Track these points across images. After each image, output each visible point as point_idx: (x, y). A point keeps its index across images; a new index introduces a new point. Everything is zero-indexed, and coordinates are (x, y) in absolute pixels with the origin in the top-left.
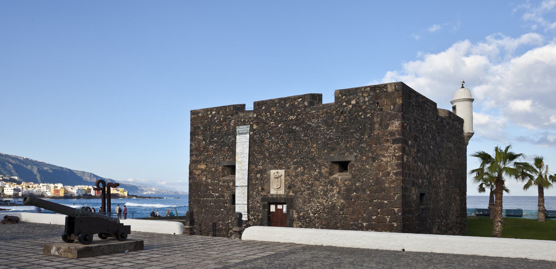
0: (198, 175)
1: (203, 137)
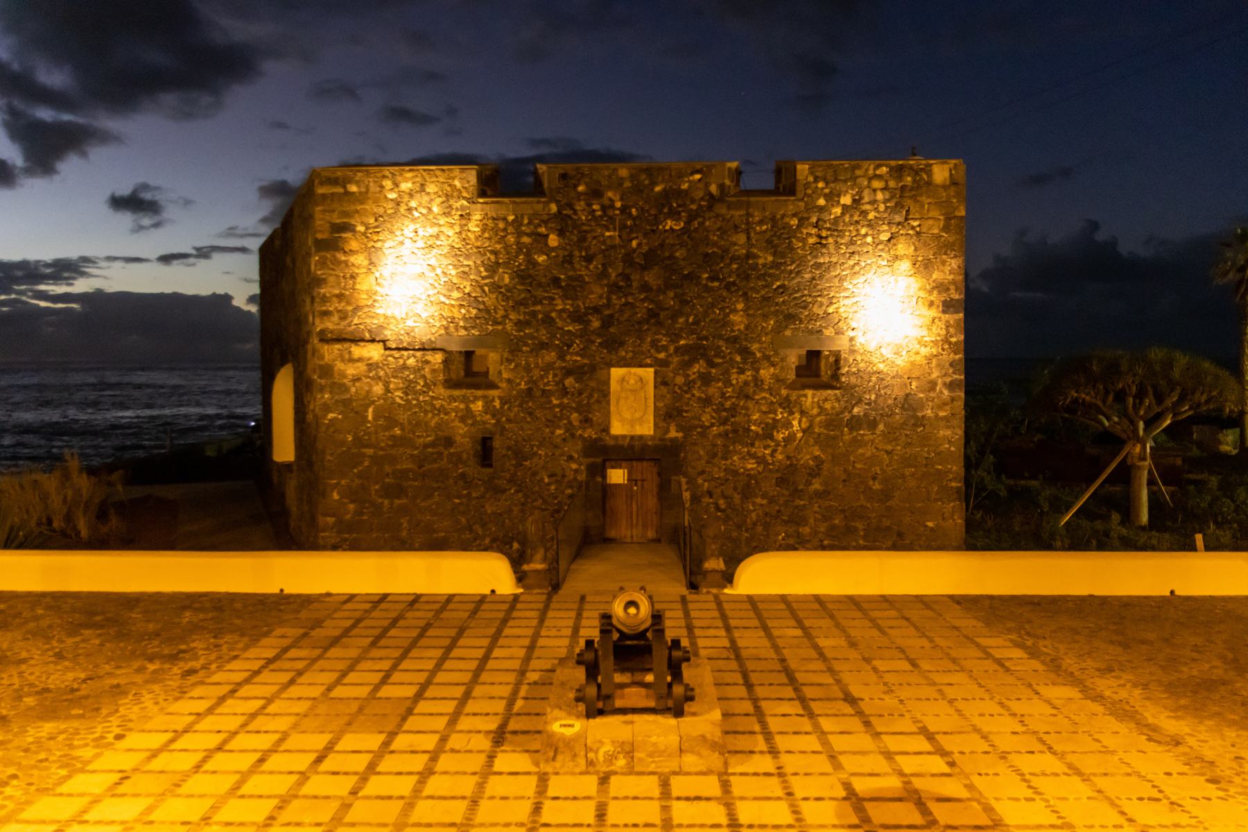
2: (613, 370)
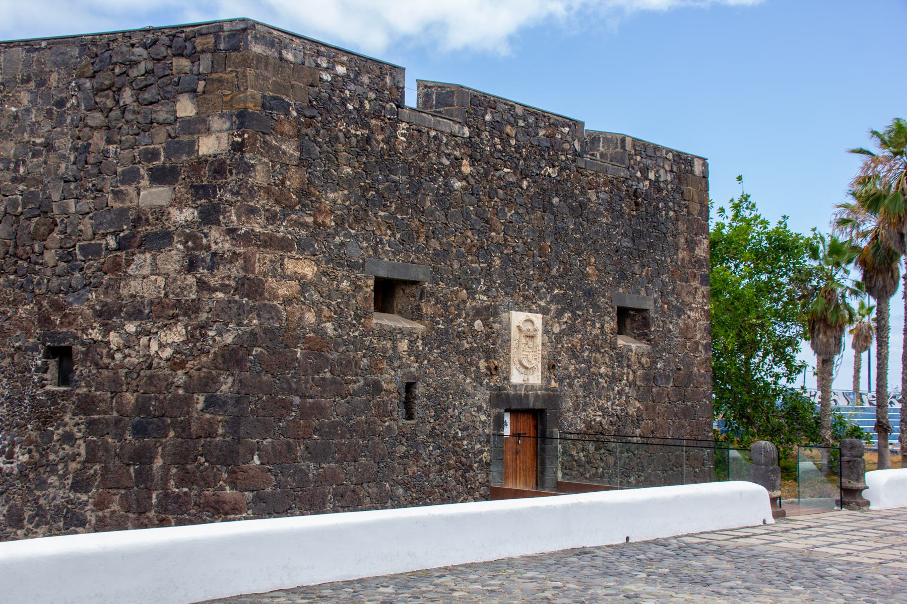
0: (288, 301)
1: (300, 148)
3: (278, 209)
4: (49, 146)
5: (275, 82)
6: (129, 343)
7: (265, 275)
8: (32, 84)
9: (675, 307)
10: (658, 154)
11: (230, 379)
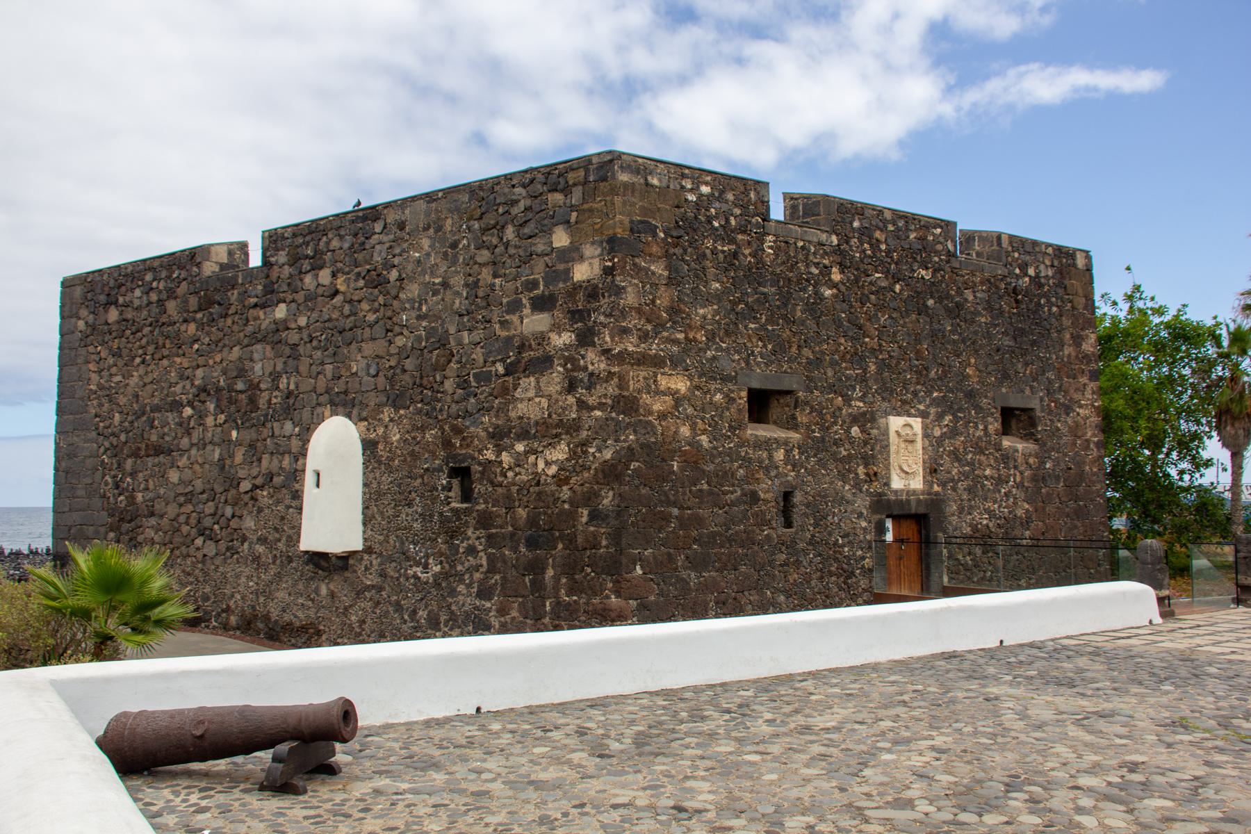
0: (662, 416)
1: (669, 267)
2: (891, 418)
3: (649, 327)
4: (445, 285)
5: (642, 208)
6: (519, 462)
7: (639, 392)
8: (432, 230)
9: (1063, 404)
10: (1037, 249)
11: (611, 494)
